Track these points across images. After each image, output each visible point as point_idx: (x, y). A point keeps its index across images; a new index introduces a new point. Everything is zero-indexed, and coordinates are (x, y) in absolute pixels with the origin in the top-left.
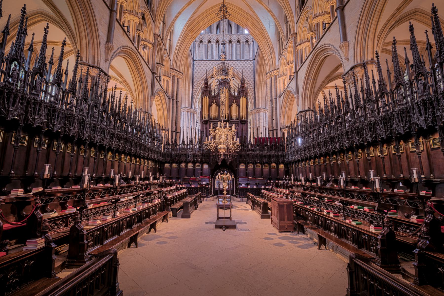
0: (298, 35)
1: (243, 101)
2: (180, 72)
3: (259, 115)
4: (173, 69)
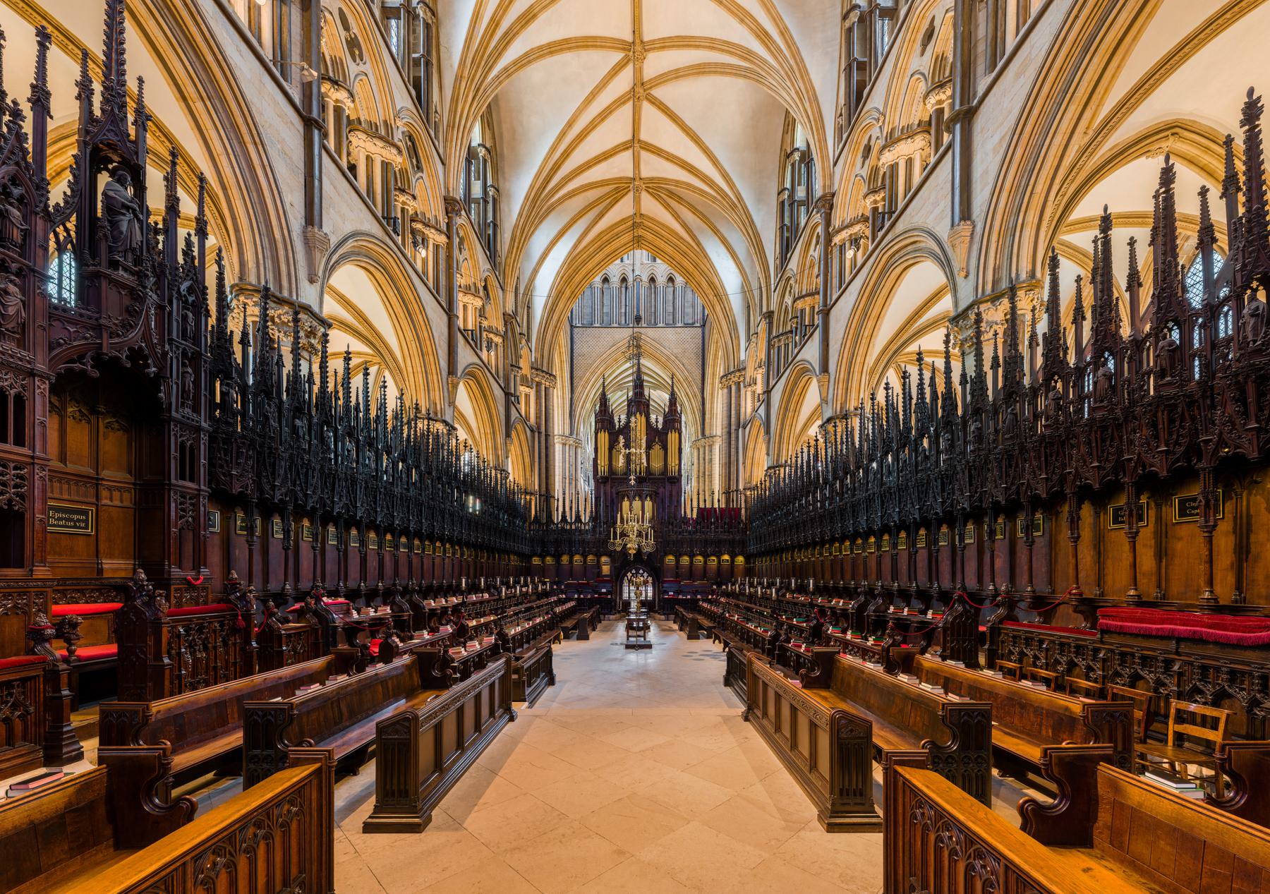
1: (672, 437)
4: (537, 370)
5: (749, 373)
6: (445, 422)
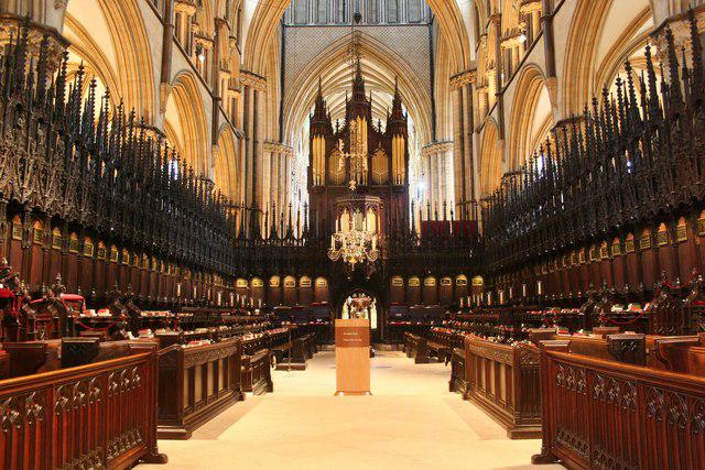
0: (504, 19)
1: (398, 142)
2: (261, 78)
3: (443, 159)
4: (246, 72)
5: (481, 73)
6: (155, 129)
